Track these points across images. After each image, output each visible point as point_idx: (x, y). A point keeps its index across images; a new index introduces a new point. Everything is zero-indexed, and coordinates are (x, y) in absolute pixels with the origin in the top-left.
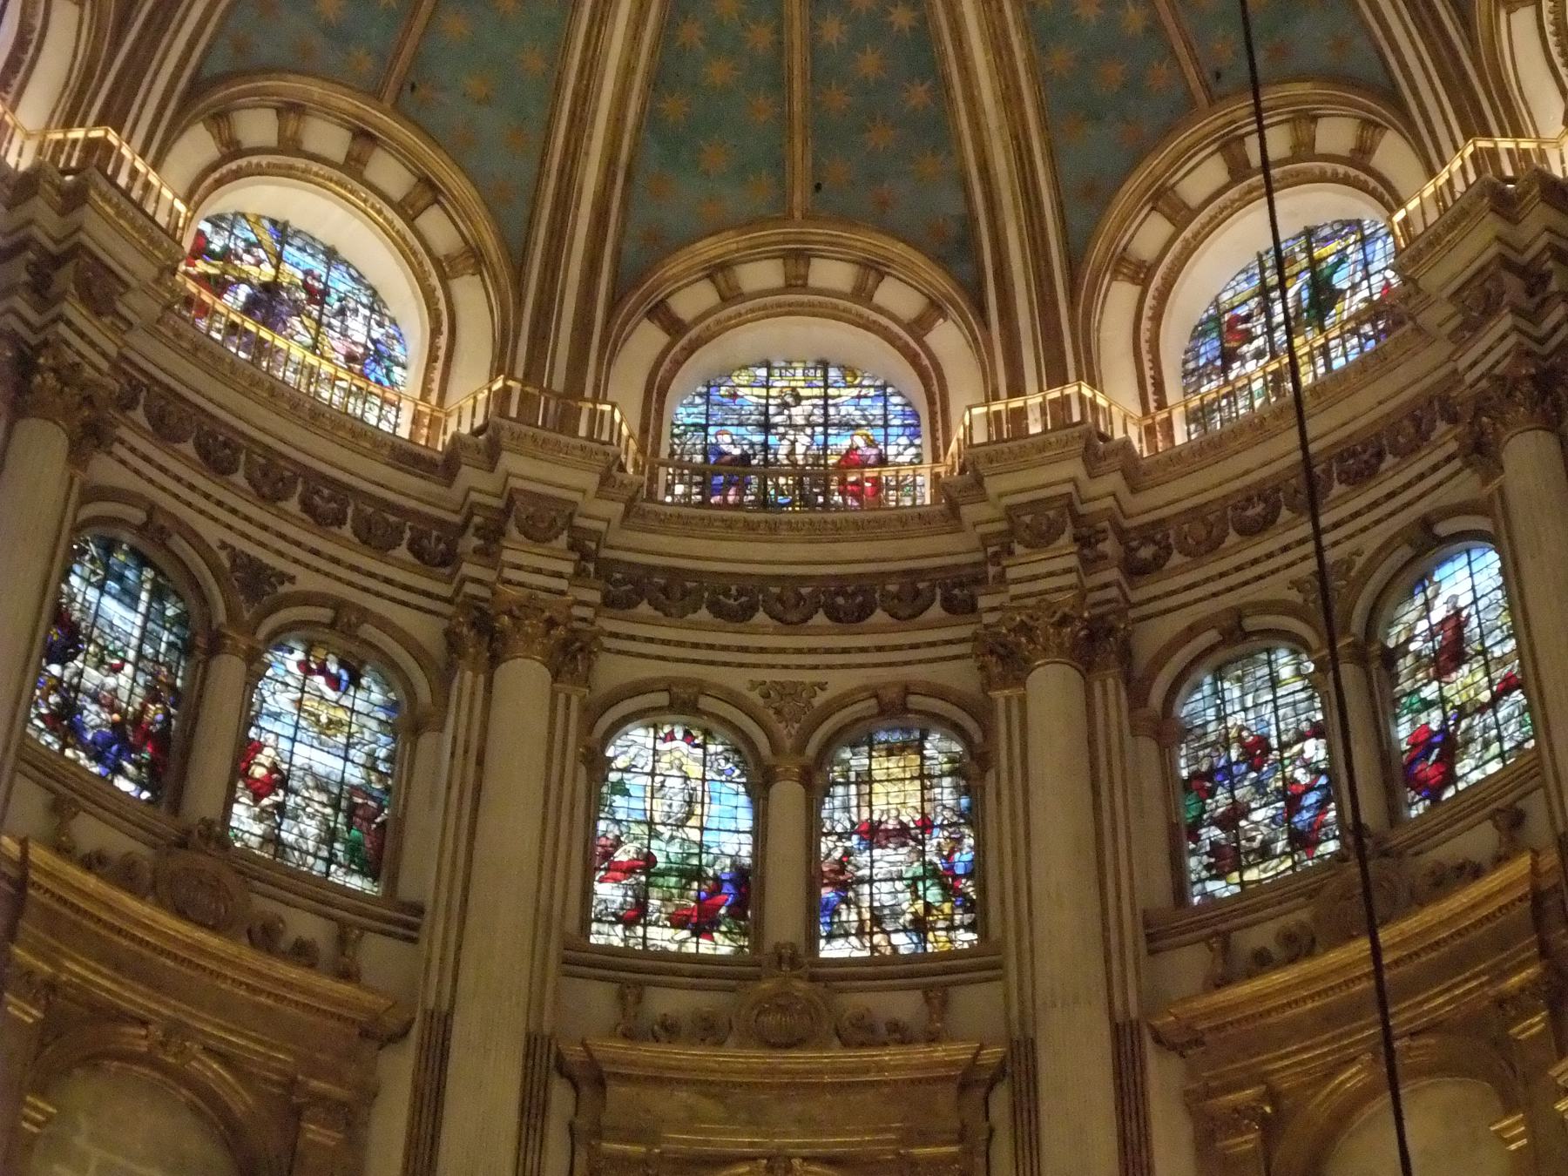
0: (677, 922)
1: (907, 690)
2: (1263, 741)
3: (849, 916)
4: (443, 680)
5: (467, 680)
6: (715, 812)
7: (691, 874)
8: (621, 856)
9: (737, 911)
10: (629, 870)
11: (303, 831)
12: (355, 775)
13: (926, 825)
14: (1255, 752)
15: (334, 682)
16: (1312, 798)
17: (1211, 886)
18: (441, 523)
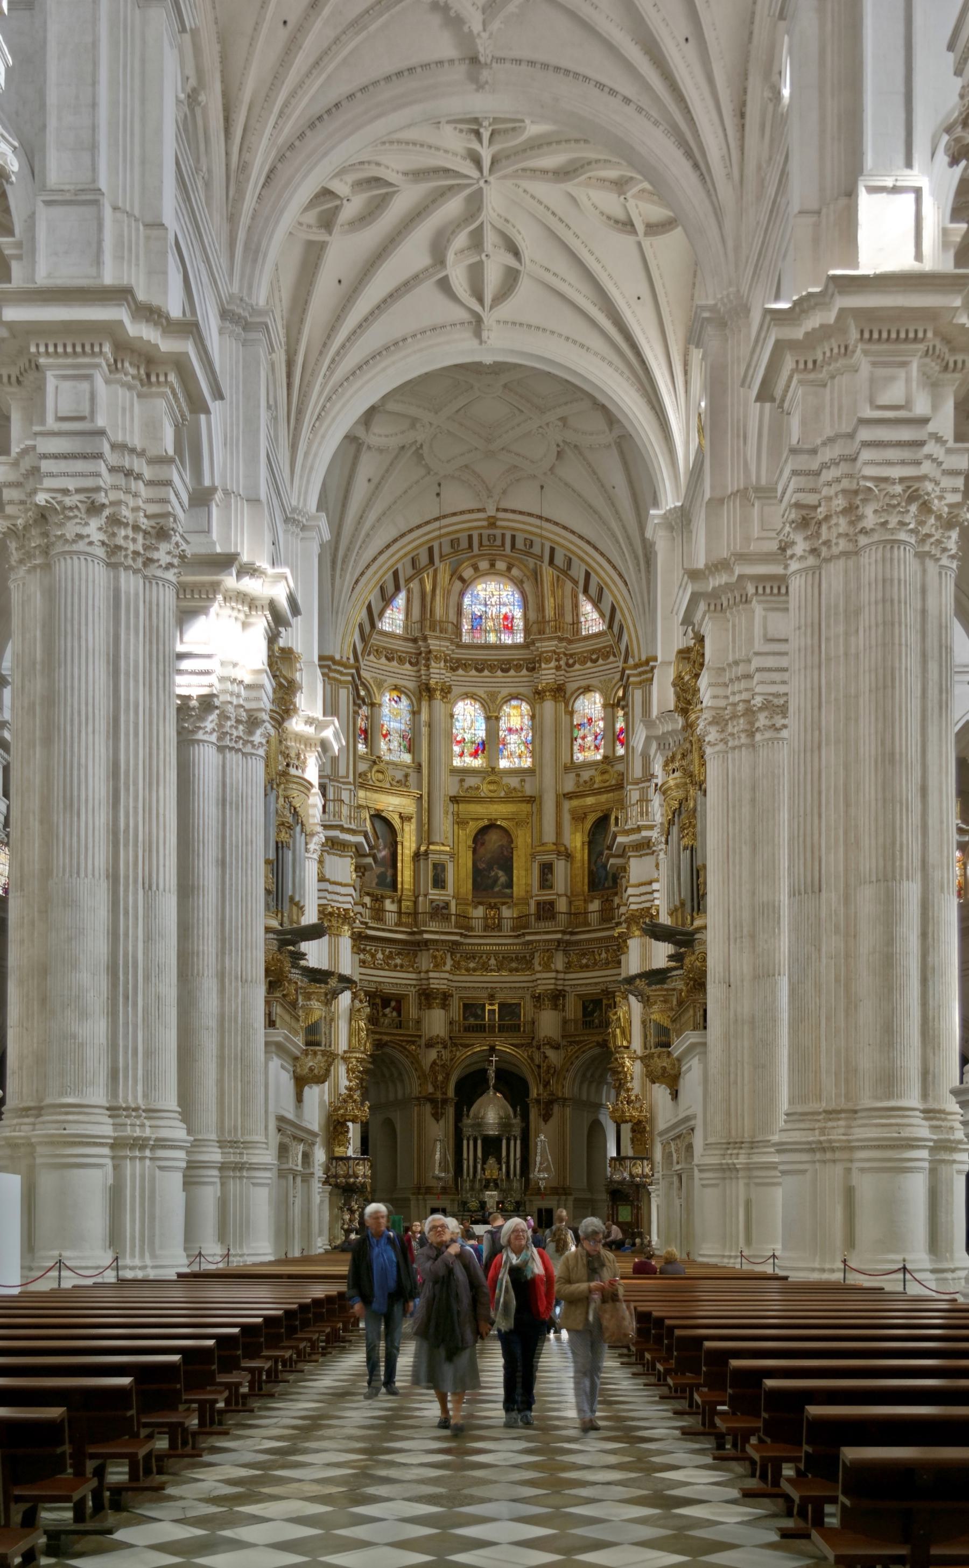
0: (471, 755)
1: (519, 694)
2: (591, 719)
3: (505, 753)
4: (419, 700)
5: (425, 705)
6: (477, 725)
7: (473, 743)
8: (458, 739)
9: (483, 752)
10: (459, 742)
11: (394, 745)
12: (403, 727)
13: (522, 729)
14: (590, 720)
15: (396, 702)
16: (599, 737)
17: (579, 755)
18: (415, 654)
